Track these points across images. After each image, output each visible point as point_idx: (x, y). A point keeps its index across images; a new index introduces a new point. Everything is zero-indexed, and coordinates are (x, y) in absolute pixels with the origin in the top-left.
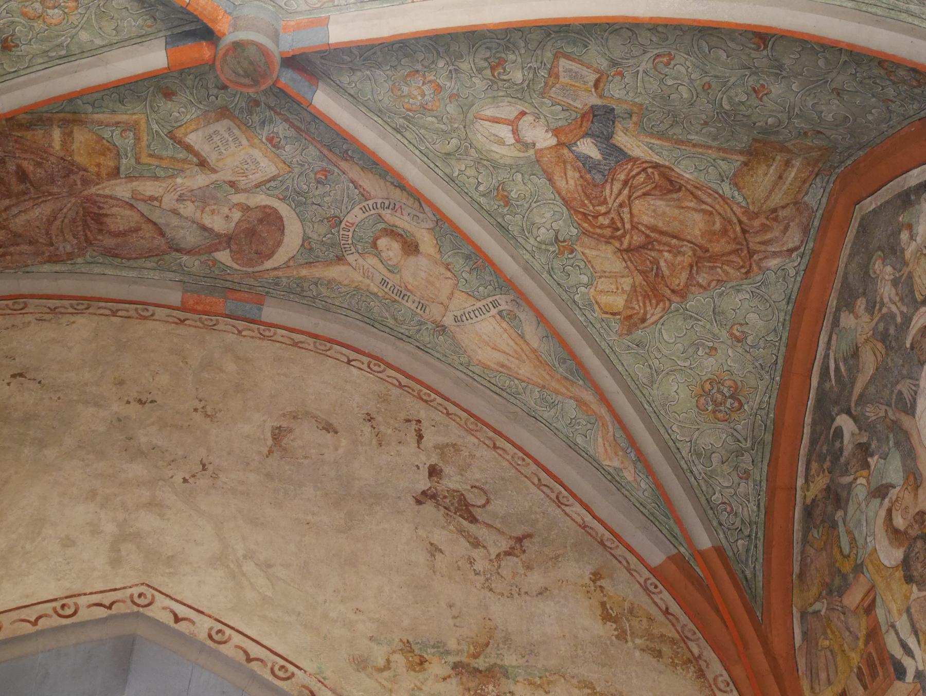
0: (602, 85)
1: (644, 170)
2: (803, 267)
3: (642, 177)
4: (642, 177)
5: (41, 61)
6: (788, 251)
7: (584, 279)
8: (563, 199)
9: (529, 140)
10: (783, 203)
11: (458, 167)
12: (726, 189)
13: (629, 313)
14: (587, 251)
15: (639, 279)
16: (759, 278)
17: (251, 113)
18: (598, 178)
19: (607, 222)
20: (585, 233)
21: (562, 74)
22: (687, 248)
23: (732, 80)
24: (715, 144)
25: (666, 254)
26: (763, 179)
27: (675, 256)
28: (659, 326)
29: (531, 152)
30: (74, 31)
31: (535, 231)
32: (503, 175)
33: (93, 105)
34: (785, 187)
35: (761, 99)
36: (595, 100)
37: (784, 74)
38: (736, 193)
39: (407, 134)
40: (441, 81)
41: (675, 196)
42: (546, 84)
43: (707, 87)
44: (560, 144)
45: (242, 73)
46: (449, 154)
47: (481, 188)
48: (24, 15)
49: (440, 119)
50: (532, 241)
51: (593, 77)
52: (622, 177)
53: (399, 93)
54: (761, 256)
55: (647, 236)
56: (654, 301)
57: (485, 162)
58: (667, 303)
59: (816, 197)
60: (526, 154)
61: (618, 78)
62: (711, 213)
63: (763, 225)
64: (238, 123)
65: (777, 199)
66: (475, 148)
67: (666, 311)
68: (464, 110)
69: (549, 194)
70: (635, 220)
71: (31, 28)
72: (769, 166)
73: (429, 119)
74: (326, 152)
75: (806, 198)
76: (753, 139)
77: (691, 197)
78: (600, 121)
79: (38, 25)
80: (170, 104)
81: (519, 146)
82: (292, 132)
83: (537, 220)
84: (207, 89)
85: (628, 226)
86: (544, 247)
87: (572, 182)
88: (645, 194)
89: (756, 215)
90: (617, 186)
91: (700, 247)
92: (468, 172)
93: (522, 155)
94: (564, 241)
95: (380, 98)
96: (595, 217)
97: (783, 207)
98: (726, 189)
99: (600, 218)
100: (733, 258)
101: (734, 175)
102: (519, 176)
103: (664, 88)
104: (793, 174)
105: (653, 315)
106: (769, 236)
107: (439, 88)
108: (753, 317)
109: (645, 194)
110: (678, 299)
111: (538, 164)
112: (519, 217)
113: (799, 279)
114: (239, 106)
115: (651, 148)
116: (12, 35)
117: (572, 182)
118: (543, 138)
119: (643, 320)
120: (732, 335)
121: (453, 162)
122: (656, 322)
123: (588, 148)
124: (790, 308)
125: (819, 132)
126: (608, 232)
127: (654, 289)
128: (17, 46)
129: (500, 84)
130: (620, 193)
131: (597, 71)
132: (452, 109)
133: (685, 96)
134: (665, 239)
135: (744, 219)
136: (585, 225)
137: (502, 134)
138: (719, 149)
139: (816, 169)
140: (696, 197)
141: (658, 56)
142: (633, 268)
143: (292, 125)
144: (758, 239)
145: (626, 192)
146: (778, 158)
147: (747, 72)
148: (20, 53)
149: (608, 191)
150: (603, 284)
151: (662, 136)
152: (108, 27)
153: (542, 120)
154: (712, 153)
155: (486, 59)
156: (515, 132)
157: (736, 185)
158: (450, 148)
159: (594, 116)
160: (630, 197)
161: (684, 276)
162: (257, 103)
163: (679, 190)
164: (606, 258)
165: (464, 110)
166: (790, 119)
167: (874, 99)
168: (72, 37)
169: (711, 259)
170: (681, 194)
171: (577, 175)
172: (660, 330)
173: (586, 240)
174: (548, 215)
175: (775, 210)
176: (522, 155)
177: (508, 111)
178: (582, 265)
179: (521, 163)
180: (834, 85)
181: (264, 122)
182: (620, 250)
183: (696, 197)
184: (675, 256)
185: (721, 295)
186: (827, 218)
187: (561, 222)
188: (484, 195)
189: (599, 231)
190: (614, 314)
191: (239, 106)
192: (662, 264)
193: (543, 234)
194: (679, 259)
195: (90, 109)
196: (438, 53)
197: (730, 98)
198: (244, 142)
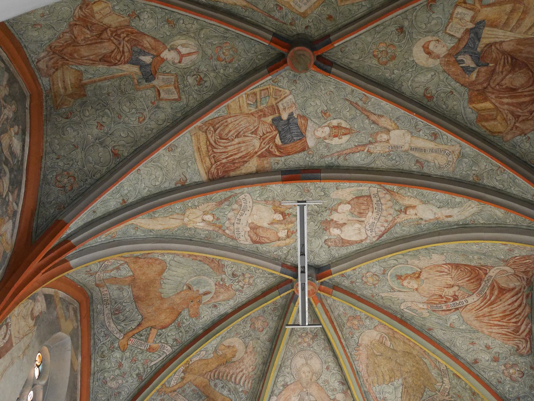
0: (157, 94)
1: (119, 61)
2: (30, 59)
3: (118, 58)
4: (118, 58)
5: (387, 23)
6: (40, 61)
7: (117, 8)
8: (145, 34)
9: (172, 51)
10: (55, 73)
11: (196, 26)
12: (82, 68)
13: (89, 7)
14: (123, 19)
15: (94, 21)
16: (44, 48)
17: (293, 19)
18: (136, 49)
19: (122, 35)
20: (128, 26)
21: (174, 90)
22: (83, 43)
23: (113, 125)
24: (99, 84)
25: (89, 36)
26: (70, 78)
27: (85, 38)
28: (72, 10)
29: (168, 47)
30: (373, 41)
31: (149, 14)
32: (175, 31)
33: (362, 6)
34: (59, 79)
35: (98, 122)
36: (155, 83)
37: (97, 141)
38: (76, 68)
39: (222, 30)
40: (219, 63)
41: (100, 57)
42: (178, 82)
43: (120, 117)
44: (158, 55)
45: (302, 56)
46: (202, 29)
47: (181, 21)
48: (394, 46)
49: (212, 44)
50: (148, 10)
51: (163, 95)
52: (126, 54)
53: (233, 49)
54: (49, 54)
55: (102, 39)
56: (81, 17)
57: (185, 33)
58: (75, 19)
59: (45, 81)
60: (170, 45)
61: (153, 101)
62: (81, 58)
63: (58, 63)
64: (297, 12)
65: (59, 73)
66: (192, 37)
67: (74, 16)
68: (204, 53)
69: (153, 34)
70: (111, 42)
71: (391, 40)
72: (71, 84)
73: (216, 42)
74: (254, 8)
75: (48, 79)
76: (85, 95)
77: (94, 59)
78: (149, 74)
79: (388, 42)
80: (329, 13)
81: (175, 47)
82: (273, 14)
83: (151, 21)
84: (314, 25)
85: (112, 38)
86: (142, 10)
87: (145, 42)
88: (112, 52)
89: (62, 65)
90: (126, 49)
91: (77, 46)
92: (190, 25)
93: (172, 43)
94: (135, 18)
95: (240, 44)
96: (128, 35)
97: (54, 72)
98: (82, 68)
99: (125, 35)
100: (61, 49)
101: (82, 74)
102: (168, 34)
103: (134, 107)
104: (60, 85)
105: (78, 12)
106: (52, 61)
107: (218, 59)
108: (36, 34)
109: (112, 52)
110: (71, 23)
111: (163, 43)
112: (160, 17)
113: (28, 55)
114: (298, 20)
115: (122, 70)
116: (399, 35)
117: (145, 42)
118: (167, 55)
119: (81, 8)
120: (39, 25)
121: (199, 27)
122: (75, 10)
123: (147, 59)
124: (23, 45)
125: (67, 118)
126: (119, 32)
127: (84, 21)
128: (397, 30)
129: (195, 73)
130: (123, 47)
131: (162, 100)
132: (209, 52)
133: (124, 107)
134: (94, 41)
135: (67, 62)
136: (130, 30)
137: (184, 49)
138: (95, 82)
139: (52, 91)
140: (92, 60)
141: (144, 120)
142: (99, 23)
143: (273, 17)
144: (55, 59)
145: (121, 49)
146: (71, 89)
147: (110, 132)
148: (396, 26)
149: (128, 45)
150: (107, 10)
151: (121, 77)
152: (360, 45)
153: (171, 63)
154: (96, 79)
155: (205, 81)
156: (179, 53)
157: (79, 71)
158: (203, 32)
159: (152, 74)
160: (118, 48)
161: (76, 32)
162: (291, 24)
163: (100, 60)
164: (113, 21)
165: (204, 53)
166: (82, 119)
167: (62, 154)
168: (374, 38)
169: (70, 44)
170: (98, 59)
171: (145, 46)
172: (71, 8)
173: (126, 23)
174: (148, 26)
175: (57, 70)
176: (172, 43)
177: (186, 61)
178: (121, 13)
179: (170, 40)
180: (79, 150)
181: (286, 16)
182: (110, 27)
183: (92, 60)
184: (85, 38)
185: (55, 34)
186: (35, 79)
187: (141, 25)
188: (179, 19)
189: (123, 30)
190: (94, 3)
191: (298, 20)
192: (88, 32)
193: (145, 16)
194: (83, 38)
195: (363, 3)
196: (225, 75)
197: (108, 116)
198: (292, 4)
